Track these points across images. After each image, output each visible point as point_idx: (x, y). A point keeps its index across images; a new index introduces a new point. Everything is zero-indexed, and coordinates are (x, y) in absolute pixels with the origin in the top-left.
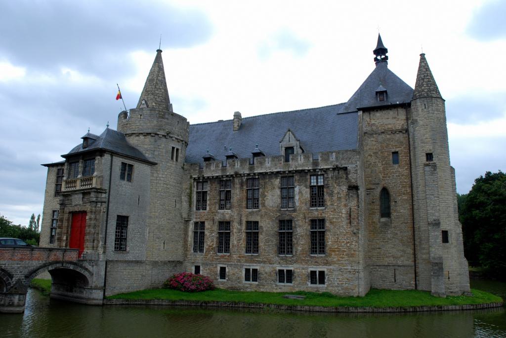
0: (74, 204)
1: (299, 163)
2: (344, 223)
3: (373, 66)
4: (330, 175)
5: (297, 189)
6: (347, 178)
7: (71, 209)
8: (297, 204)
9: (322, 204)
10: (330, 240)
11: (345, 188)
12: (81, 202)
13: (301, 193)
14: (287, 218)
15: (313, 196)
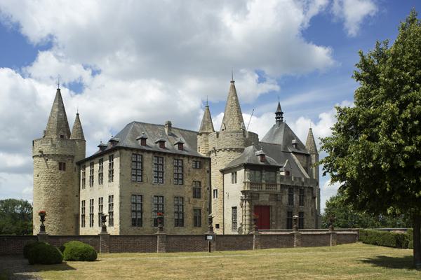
0: (260, 200)
1: (297, 183)
2: (310, 215)
3: (274, 122)
4: (306, 190)
5: (295, 195)
6: (312, 193)
7: (257, 204)
8: (295, 204)
9: (303, 205)
10: (305, 221)
11: (311, 197)
12: (267, 199)
13: (296, 197)
14: (290, 211)
15: (300, 200)
